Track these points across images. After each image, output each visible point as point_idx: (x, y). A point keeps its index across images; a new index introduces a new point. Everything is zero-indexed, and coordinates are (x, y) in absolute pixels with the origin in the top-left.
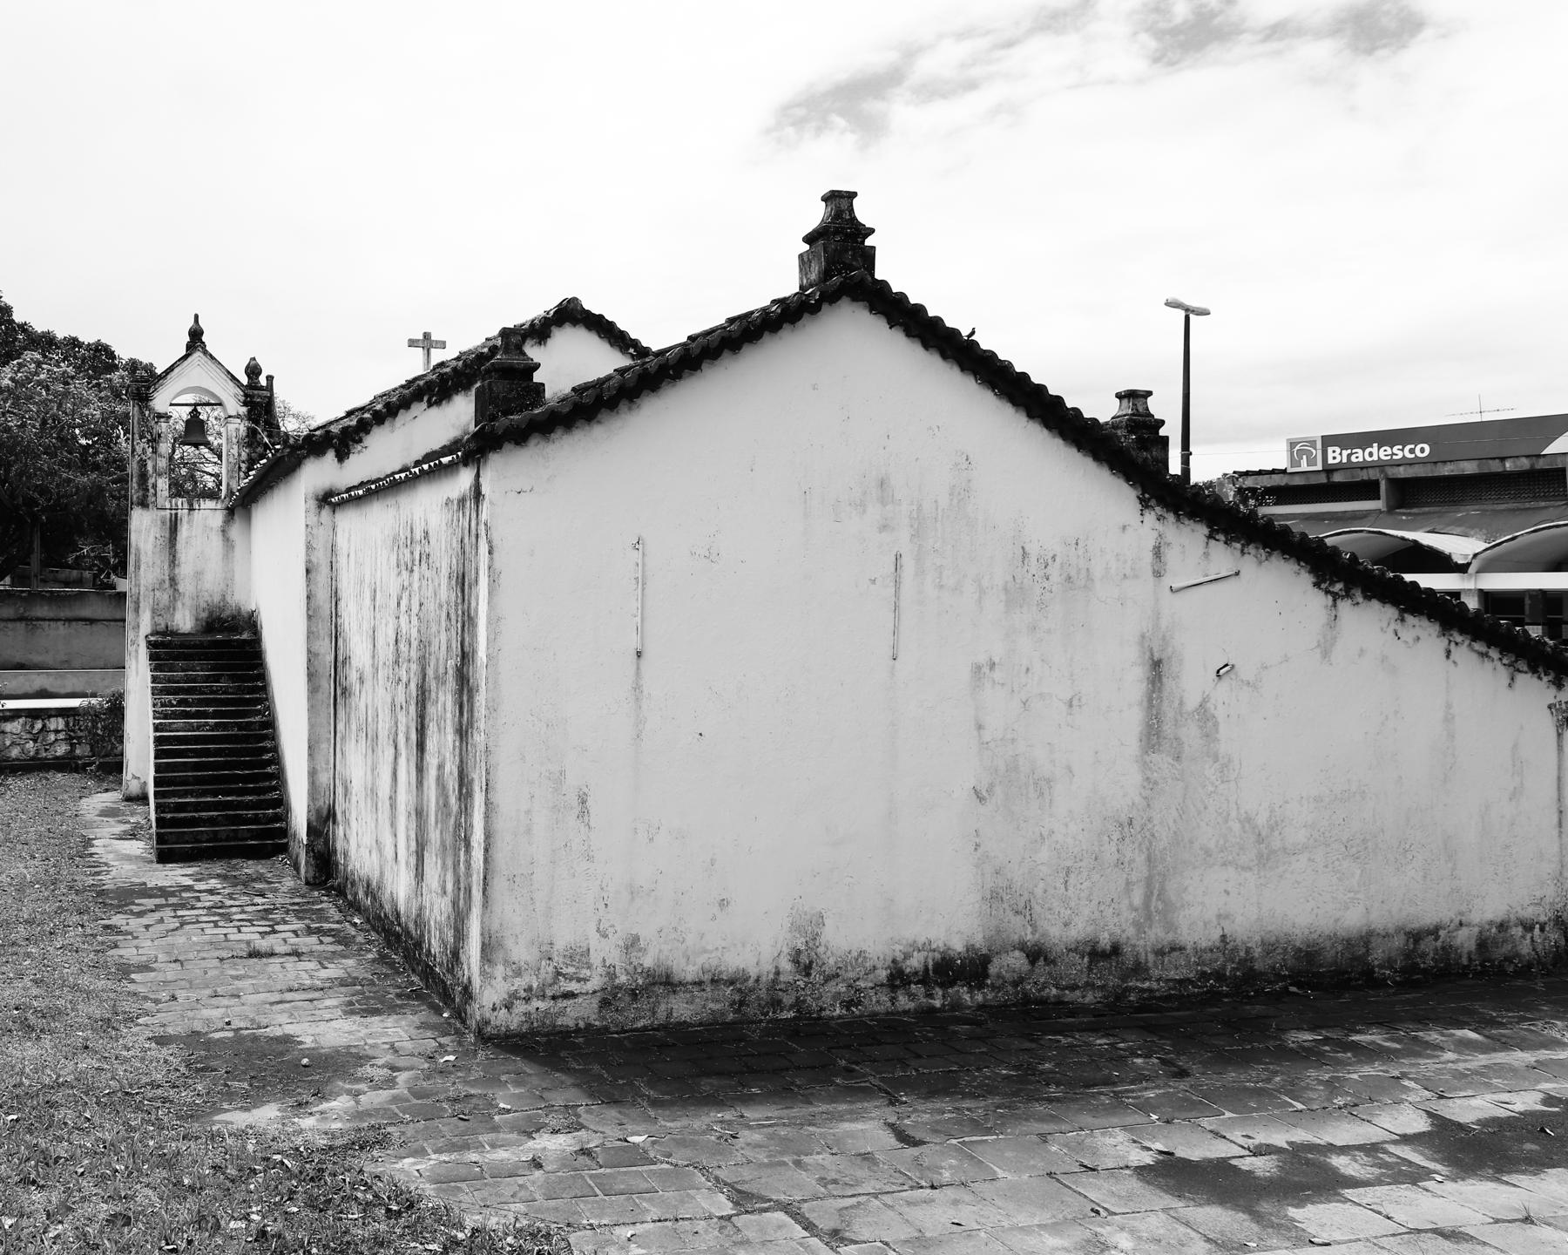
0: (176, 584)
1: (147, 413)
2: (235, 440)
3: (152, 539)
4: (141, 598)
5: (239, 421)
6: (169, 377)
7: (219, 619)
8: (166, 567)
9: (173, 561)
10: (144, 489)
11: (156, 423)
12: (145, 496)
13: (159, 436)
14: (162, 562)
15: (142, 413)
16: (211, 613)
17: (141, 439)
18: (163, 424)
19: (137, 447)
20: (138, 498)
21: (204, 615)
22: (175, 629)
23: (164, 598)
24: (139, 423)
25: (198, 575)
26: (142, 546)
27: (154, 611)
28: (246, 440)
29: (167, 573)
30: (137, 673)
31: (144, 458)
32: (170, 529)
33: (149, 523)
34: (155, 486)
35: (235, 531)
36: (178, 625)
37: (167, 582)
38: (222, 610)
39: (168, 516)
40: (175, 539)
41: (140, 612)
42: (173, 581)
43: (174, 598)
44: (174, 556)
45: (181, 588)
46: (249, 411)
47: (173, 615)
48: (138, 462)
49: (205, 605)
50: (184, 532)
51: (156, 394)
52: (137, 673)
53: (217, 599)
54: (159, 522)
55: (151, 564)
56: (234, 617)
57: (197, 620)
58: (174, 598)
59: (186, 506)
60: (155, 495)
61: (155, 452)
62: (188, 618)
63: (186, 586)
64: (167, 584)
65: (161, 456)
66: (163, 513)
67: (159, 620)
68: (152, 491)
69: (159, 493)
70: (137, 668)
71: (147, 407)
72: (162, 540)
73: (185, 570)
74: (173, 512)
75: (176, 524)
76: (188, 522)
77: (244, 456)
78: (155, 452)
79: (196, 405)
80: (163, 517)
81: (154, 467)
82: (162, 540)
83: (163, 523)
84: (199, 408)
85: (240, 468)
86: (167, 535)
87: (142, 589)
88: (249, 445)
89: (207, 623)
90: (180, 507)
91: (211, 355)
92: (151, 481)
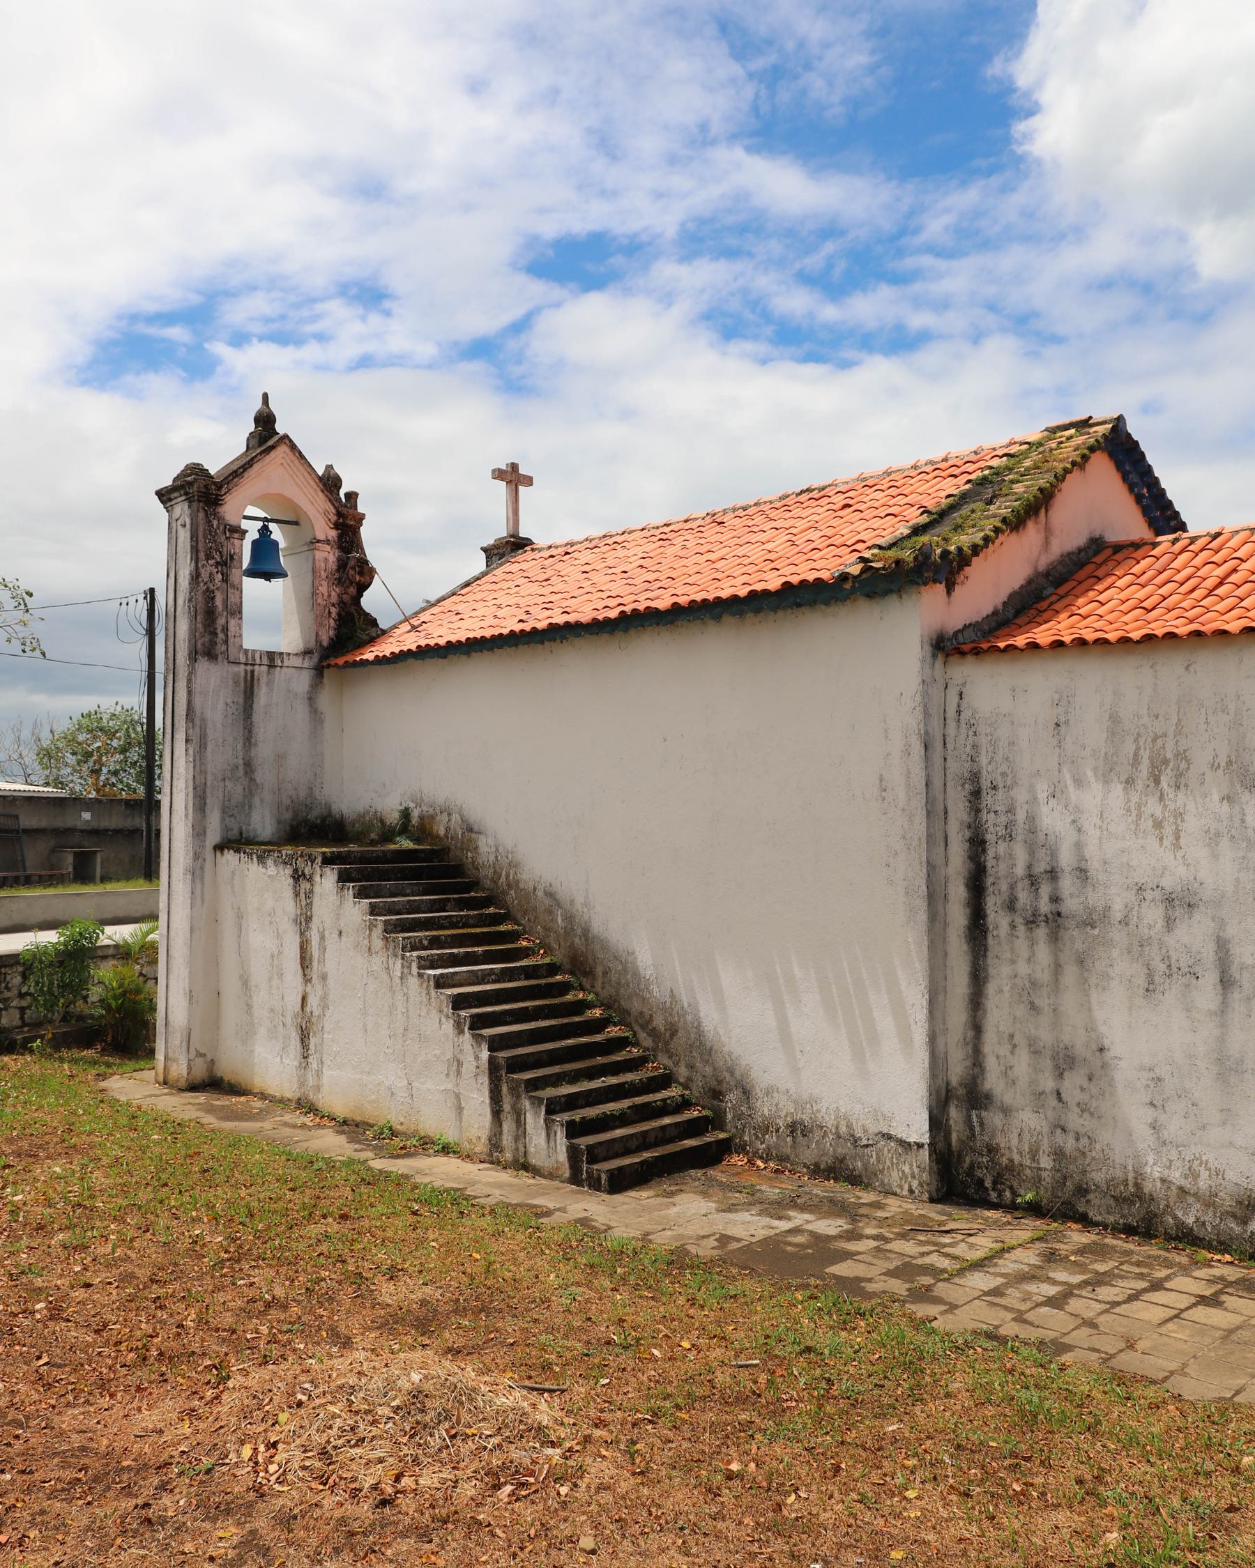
0: (252, 772)
1: (215, 523)
2: (324, 575)
3: (221, 706)
4: (208, 790)
5: (328, 548)
6: (246, 474)
7: (306, 821)
8: (240, 747)
9: (249, 738)
12: (213, 643)
13: (232, 558)
14: (235, 739)
16: (296, 814)
17: (207, 559)
18: (236, 542)
19: (202, 571)
20: (203, 644)
21: (288, 816)
22: (252, 835)
23: (237, 790)
25: (280, 758)
26: (209, 714)
27: (224, 811)
28: (337, 576)
29: (241, 754)
30: (203, 900)
32: (245, 692)
34: (225, 629)
35: (325, 700)
36: (255, 830)
37: (241, 768)
38: (309, 808)
39: (242, 674)
40: (251, 707)
41: (207, 811)
42: (249, 766)
43: (250, 791)
44: (250, 732)
45: (259, 777)
46: (340, 537)
47: (249, 815)
48: (204, 593)
49: (288, 802)
50: (262, 697)
52: (203, 900)
53: (303, 793)
54: (231, 682)
55: (221, 740)
56: (324, 819)
57: (279, 822)
58: (250, 791)
59: (265, 661)
60: (226, 642)
61: (225, 580)
62: (268, 819)
63: (265, 775)
64: (241, 772)
66: (236, 669)
67: (231, 822)
68: (221, 636)
69: (231, 640)
70: (202, 893)
72: (234, 707)
73: (264, 751)
74: (249, 668)
75: (252, 686)
76: (268, 684)
77: (334, 599)
79: (265, 519)
80: (236, 675)
81: (225, 601)
82: (234, 707)
83: (236, 683)
84: (272, 526)
85: (330, 613)
86: (241, 701)
87: (209, 777)
88: (339, 582)
89: (292, 827)
90: (258, 661)
92: (221, 622)
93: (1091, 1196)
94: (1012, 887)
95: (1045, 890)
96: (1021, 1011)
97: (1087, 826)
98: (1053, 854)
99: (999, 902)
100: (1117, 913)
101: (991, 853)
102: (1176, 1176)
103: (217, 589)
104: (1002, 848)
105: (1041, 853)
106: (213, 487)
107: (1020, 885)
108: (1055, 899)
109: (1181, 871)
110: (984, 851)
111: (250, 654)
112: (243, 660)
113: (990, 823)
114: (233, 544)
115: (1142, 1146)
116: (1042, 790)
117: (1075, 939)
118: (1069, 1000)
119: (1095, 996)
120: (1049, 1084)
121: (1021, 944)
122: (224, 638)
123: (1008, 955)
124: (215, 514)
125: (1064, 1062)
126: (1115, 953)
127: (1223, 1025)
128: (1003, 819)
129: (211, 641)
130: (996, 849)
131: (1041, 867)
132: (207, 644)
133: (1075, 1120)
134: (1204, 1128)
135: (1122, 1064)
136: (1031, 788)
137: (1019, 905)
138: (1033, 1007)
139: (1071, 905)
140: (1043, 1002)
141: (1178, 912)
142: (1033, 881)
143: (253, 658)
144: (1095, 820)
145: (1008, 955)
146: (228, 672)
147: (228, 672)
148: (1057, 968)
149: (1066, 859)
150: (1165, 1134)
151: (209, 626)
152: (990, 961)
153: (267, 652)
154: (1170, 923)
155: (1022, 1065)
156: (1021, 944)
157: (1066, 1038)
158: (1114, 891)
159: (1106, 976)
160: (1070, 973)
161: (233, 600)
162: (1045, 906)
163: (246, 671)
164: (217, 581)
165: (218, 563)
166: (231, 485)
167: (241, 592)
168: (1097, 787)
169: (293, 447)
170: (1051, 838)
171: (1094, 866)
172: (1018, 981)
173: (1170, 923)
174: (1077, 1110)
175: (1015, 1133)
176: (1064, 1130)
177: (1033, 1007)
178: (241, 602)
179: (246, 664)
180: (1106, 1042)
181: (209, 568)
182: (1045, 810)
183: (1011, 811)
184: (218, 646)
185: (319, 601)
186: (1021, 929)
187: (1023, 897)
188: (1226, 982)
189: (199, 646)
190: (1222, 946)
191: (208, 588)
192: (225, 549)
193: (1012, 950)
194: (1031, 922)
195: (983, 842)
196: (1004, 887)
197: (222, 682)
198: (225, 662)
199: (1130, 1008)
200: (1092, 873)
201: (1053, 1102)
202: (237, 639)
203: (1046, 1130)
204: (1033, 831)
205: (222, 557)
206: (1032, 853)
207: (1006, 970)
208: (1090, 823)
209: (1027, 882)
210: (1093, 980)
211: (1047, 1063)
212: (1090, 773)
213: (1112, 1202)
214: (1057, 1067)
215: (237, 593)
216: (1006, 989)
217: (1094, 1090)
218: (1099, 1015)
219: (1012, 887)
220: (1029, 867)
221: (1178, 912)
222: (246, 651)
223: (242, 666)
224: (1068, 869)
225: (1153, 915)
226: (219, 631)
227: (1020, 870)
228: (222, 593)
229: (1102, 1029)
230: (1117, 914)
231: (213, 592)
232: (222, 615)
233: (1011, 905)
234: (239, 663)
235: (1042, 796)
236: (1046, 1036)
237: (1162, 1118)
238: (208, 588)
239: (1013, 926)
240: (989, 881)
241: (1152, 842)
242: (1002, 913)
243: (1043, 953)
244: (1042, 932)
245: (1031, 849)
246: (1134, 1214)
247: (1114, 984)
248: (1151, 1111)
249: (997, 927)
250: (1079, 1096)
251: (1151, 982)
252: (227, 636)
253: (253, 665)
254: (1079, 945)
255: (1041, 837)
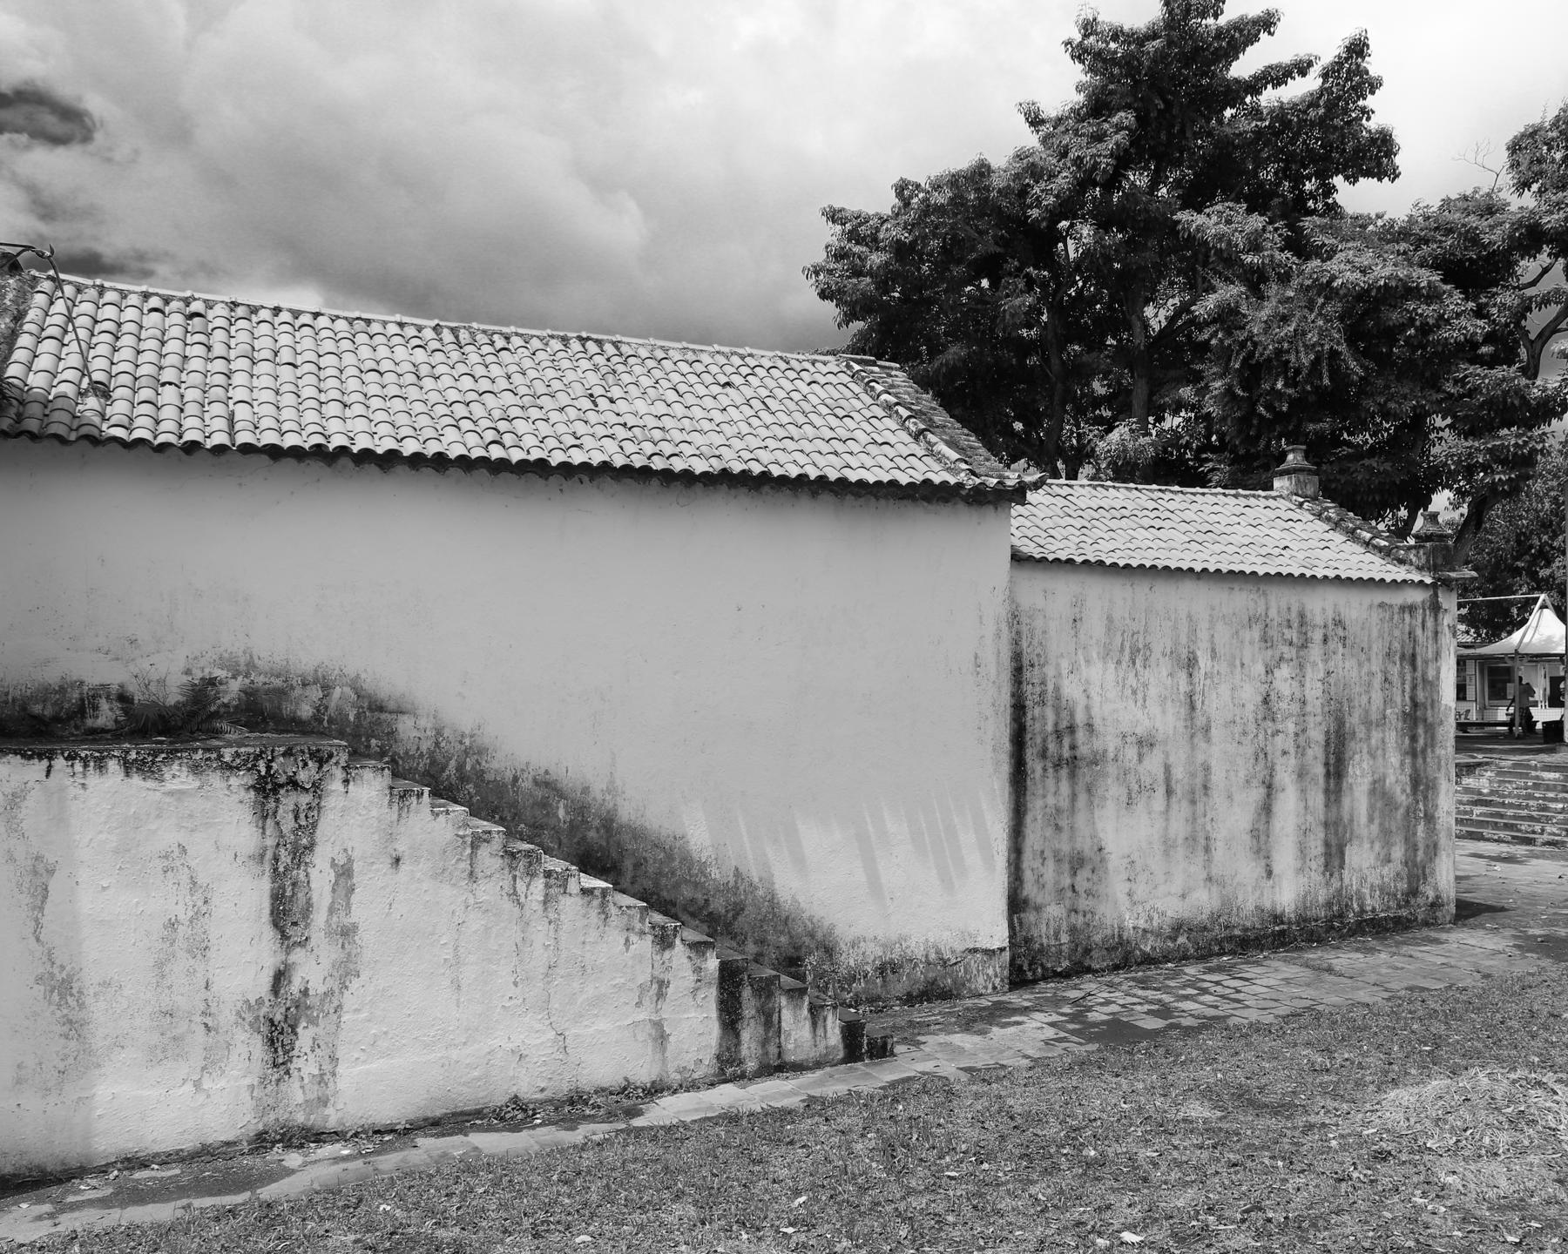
93: (1093, 953)
94: (1044, 741)
95: (1066, 742)
96: (1049, 832)
97: (1093, 694)
98: (1072, 715)
99: (1035, 751)
100: (1111, 755)
101: (1029, 716)
102: (1142, 924)
104: (1037, 711)
105: (1064, 714)
107: (1050, 739)
108: (1073, 747)
109: (1147, 723)
110: (1024, 714)
113: (1028, 693)
115: (1123, 908)
116: (1065, 665)
117: (1085, 774)
118: (1081, 819)
119: (1097, 813)
120: (1067, 881)
121: (1050, 782)
123: (1041, 792)
125: (1077, 863)
126: (1110, 781)
127: (1167, 820)
128: (1038, 690)
130: (1033, 712)
131: (1064, 724)
133: (1083, 903)
134: (1155, 888)
135: (1113, 856)
136: (1058, 665)
137: (1049, 753)
138: (1058, 828)
139: (1083, 751)
140: (1064, 823)
141: (1145, 749)
142: (1058, 734)
144: (1098, 689)
145: (1041, 792)
148: (1074, 797)
149: (1080, 718)
150: (1135, 898)
152: (1028, 798)
154: (1140, 757)
155: (1049, 872)
156: (1050, 782)
157: (1078, 846)
158: (1109, 738)
159: (1104, 798)
160: (1082, 798)
162: (1066, 753)
168: (1100, 665)
170: (1071, 703)
171: (1097, 722)
172: (1048, 810)
173: (1140, 757)
174: (1084, 895)
175: (1044, 922)
176: (1076, 912)
177: (1058, 828)
180: (1103, 844)
182: (1066, 682)
183: (1043, 683)
186: (1051, 770)
187: (1052, 747)
188: (1169, 792)
190: (1167, 769)
193: (1044, 787)
194: (1057, 766)
195: (1024, 707)
196: (1039, 740)
199: (1118, 817)
200: (1096, 726)
201: (1069, 894)
203: (1065, 915)
204: (1058, 698)
206: (1057, 714)
207: (1039, 803)
208: (1094, 691)
209: (1054, 736)
210: (1096, 802)
211: (1066, 866)
212: (1095, 656)
213: (1105, 953)
214: (1072, 868)
216: (1039, 817)
217: (1095, 878)
218: (1099, 825)
219: (1044, 741)
220: (1056, 724)
221: (1145, 749)
224: (1081, 725)
225: (1131, 753)
227: (1050, 728)
229: (1101, 835)
230: (1111, 755)
233: (1043, 754)
235: (1065, 672)
236: (1065, 848)
237: (1134, 887)
239: (1045, 770)
240: (1028, 736)
241: (1131, 703)
242: (1037, 761)
243: (1065, 787)
244: (1064, 772)
245: (1057, 710)
246: (1117, 957)
247: (1109, 802)
248: (1128, 885)
249: (1033, 772)
250: (1086, 885)
251: (1130, 798)
254: (1088, 779)
255: (1064, 702)
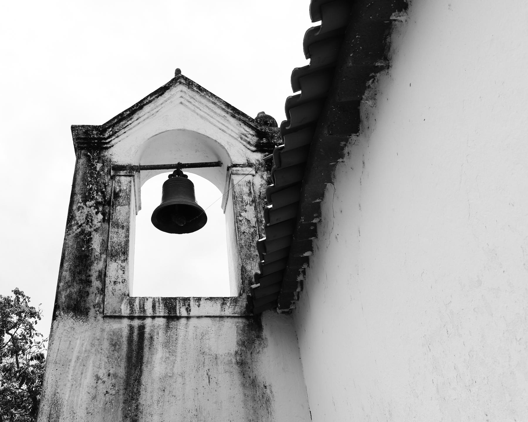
1: (99, 166)
10: (81, 281)
11: (113, 178)
12: (83, 294)
13: (116, 195)
15: (90, 165)
17: (85, 201)
18: (123, 179)
20: (69, 297)
24: (84, 179)
31: (88, 229)
33: (87, 345)
34: (102, 276)
39: (125, 332)
51: (114, 141)
54: (106, 344)
60: (102, 291)
61: (107, 219)
65: (117, 225)
66: (115, 325)
68: (96, 284)
69: (110, 287)
71: (100, 159)
74: (136, 323)
78: (107, 219)
81: (105, 244)
84: (185, 172)
90: (149, 312)
91: (199, 87)
103: (96, 230)
106: (95, 132)
111: (137, 303)
112: (125, 310)
114: (119, 182)
122: (100, 287)
124: (99, 158)
129: (80, 291)
132: (74, 296)
143: (142, 308)
146: (103, 330)
147: (103, 330)
151: (79, 273)
153: (164, 299)
161: (115, 240)
163: (131, 328)
164: (95, 222)
165: (98, 204)
166: (116, 129)
167: (128, 230)
169: (190, 83)
178: (127, 242)
179: (131, 318)
181: (86, 210)
184: (91, 297)
185: (243, 228)
189: (63, 299)
191: (82, 232)
192: (109, 189)
197: (93, 345)
198: (100, 317)
202: (119, 286)
205: (104, 196)
215: (122, 232)
222: (131, 301)
223: (126, 322)
226: (93, 278)
228: (102, 234)
231: (90, 234)
232: (98, 259)
234: (121, 317)
238: (82, 232)
252: (104, 283)
253: (143, 318)
